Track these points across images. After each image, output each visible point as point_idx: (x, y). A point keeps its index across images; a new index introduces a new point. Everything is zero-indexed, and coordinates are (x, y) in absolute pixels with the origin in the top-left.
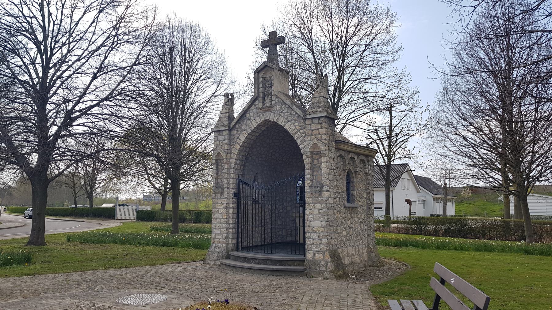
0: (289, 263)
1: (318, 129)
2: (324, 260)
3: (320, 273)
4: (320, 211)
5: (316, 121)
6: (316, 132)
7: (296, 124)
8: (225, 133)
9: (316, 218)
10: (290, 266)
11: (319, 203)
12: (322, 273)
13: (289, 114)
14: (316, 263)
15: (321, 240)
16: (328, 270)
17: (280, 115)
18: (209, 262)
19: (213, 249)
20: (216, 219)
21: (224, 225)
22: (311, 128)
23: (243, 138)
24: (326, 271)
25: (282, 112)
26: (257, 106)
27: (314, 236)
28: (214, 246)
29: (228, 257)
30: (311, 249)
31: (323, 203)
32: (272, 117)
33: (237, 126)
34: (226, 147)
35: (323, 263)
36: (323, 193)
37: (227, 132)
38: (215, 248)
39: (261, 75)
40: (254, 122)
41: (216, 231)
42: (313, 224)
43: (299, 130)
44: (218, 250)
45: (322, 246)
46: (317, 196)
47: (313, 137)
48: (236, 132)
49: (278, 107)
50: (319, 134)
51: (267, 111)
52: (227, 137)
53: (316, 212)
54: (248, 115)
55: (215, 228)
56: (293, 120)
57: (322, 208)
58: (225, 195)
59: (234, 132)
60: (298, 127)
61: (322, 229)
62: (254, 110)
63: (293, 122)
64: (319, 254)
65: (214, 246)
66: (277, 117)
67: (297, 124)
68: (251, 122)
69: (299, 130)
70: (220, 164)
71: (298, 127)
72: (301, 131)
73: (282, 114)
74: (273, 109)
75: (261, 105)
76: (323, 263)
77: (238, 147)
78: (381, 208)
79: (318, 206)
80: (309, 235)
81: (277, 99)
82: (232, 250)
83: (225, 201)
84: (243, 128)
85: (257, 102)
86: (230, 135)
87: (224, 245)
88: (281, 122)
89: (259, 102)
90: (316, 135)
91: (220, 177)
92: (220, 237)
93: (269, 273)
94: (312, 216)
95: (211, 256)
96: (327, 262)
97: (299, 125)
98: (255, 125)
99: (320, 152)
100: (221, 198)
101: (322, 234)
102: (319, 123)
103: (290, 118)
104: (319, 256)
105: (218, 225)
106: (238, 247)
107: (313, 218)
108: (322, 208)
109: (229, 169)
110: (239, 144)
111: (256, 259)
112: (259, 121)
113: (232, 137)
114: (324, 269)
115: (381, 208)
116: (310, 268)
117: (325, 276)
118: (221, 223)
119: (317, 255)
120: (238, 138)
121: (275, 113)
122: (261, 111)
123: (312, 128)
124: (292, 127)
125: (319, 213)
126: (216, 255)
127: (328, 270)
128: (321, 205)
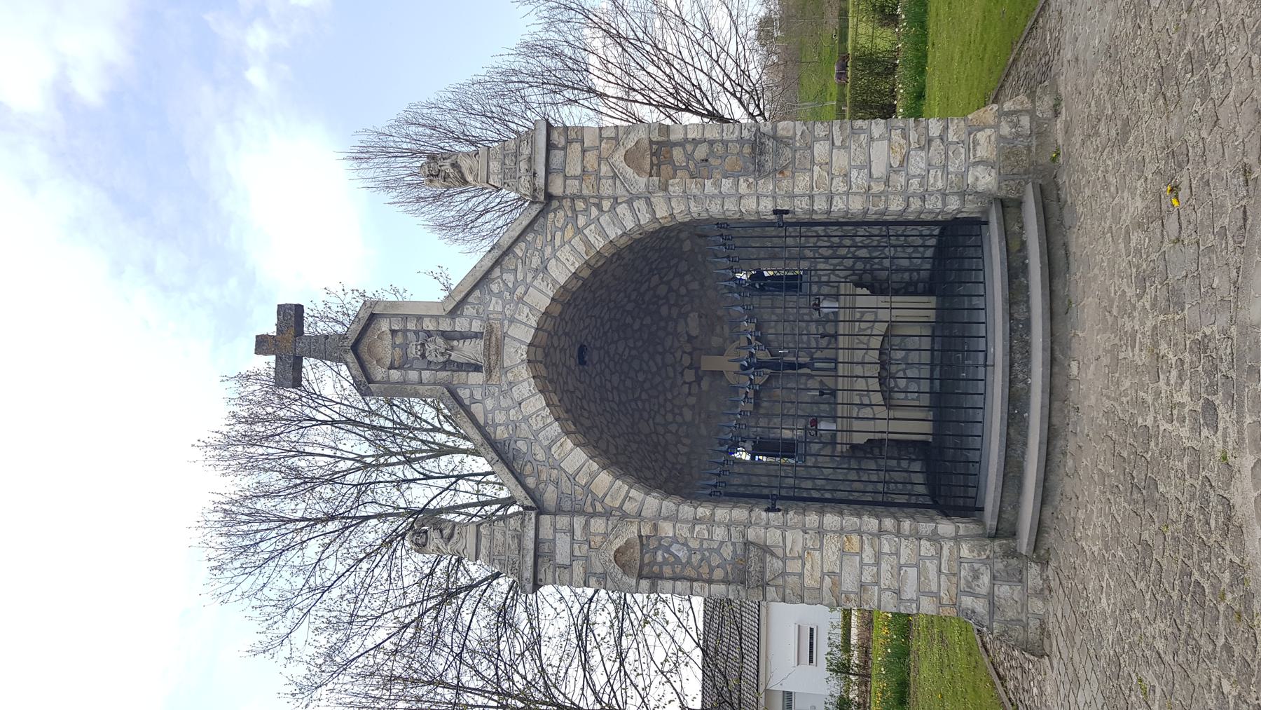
0: (1015, 246)
1: (584, 151)
2: (997, 127)
3: (1040, 132)
4: (838, 143)
5: (557, 157)
6: (591, 157)
7: (558, 242)
8: (547, 532)
9: (860, 159)
10: (1023, 244)
11: (811, 148)
12: (1039, 125)
13: (524, 263)
14: (1007, 151)
15: (930, 141)
16: (1028, 105)
17: (521, 299)
18: (1034, 624)
19: (980, 606)
20: (862, 586)
21: (886, 549)
22: (575, 177)
23: (575, 458)
24: (1031, 113)
25: (512, 293)
26: (478, 396)
27: (917, 163)
28: (967, 601)
29: (1005, 531)
30: (963, 176)
31: (812, 132)
32: (522, 333)
33: (531, 482)
34: (598, 525)
35: (1006, 130)
36: (780, 133)
37: (546, 520)
38: (976, 596)
39: (379, 373)
40: (523, 405)
41: (910, 592)
42: (879, 169)
43: (578, 231)
44: (985, 579)
45: (952, 137)
46: (788, 152)
47: (605, 169)
48: (551, 488)
49: (495, 306)
50: (598, 148)
51: (499, 352)
52: (563, 521)
53: (840, 160)
54: (501, 434)
55: (898, 592)
56: (542, 251)
57: (829, 138)
58: (774, 537)
59: (550, 496)
60: (569, 232)
61: (896, 136)
62: (489, 403)
63: (549, 250)
64: (976, 143)
65: (967, 601)
66: (526, 310)
67: (558, 234)
68: (526, 419)
69: (578, 231)
70: (656, 569)
71: (569, 232)
72: (582, 221)
73: (520, 290)
74: (496, 325)
75: (476, 378)
76: (1006, 130)
77: (605, 478)
78: (812, 630)
79: (820, 149)
80: (915, 181)
81: (469, 310)
82: (981, 522)
83: (795, 541)
84: (541, 456)
85: (464, 394)
86: (559, 511)
87: (965, 552)
88: (541, 297)
89: (465, 385)
90: (600, 158)
91: (705, 570)
92: (931, 567)
93: (1058, 284)
94: (854, 173)
95: (1010, 614)
96: (1001, 114)
97: (563, 229)
99: (651, 142)
100: (784, 560)
101: (913, 136)
102: (564, 148)
103: (535, 262)
104: (985, 145)
105: (886, 580)
107: (861, 168)
108: (829, 138)
109: (674, 519)
110: (593, 476)
111: (1011, 366)
113: (567, 505)
114: (1025, 121)
115: (812, 630)
116: (1026, 172)
117: (1049, 114)
118: (877, 563)
119: (983, 151)
120: (572, 478)
121: (512, 321)
122: (496, 375)
123: (578, 172)
125: (843, 147)
126: (1003, 591)
127: (1028, 105)
128: (818, 140)
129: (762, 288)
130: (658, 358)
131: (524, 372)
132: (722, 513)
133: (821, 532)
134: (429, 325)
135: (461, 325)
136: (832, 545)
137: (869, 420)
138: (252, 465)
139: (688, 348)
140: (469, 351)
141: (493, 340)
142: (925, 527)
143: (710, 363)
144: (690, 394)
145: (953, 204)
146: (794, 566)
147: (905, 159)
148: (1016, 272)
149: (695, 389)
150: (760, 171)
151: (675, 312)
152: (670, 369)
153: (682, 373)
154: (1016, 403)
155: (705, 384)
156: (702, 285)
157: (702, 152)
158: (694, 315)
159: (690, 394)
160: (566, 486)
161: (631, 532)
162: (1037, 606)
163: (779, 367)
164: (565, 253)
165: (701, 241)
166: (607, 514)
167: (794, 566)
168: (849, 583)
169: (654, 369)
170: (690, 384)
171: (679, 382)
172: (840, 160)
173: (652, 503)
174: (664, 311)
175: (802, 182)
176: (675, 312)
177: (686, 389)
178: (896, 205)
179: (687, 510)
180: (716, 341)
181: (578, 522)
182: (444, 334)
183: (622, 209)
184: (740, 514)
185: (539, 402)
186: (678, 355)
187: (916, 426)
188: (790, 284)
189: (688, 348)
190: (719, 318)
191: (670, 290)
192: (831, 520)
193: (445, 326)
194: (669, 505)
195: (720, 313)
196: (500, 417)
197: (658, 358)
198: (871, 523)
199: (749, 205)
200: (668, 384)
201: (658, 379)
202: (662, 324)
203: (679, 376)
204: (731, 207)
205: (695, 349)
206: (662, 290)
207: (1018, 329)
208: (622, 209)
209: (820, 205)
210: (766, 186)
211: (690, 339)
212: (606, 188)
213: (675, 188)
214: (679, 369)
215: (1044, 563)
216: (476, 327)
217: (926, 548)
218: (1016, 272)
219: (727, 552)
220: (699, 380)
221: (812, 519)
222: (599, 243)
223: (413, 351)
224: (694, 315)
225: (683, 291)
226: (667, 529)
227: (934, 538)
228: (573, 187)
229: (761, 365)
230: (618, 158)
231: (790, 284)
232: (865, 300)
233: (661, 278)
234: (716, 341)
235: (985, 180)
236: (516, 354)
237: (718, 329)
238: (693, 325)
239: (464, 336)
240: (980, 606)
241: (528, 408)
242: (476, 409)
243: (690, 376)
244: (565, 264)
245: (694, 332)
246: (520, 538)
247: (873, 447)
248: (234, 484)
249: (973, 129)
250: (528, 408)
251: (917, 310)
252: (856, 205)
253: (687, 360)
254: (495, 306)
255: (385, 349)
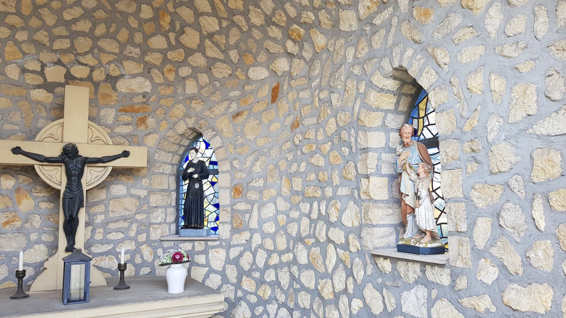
129: (186, 176)
130: (84, 26)
139: (98, 75)
143: (77, 99)
144: (24, 71)
149: (30, 79)
151: (154, 58)
152: (65, 44)
153: (59, 62)
155: (40, 95)
156: (192, 98)
158: (147, 86)
159: (24, 71)
163: (71, 205)
165: (266, 92)
169: (67, 16)
170: (42, 73)
171: (46, 57)
174: (158, 42)
176: (154, 58)
177: (35, 66)
180: (109, 115)
186: (89, 60)
188: (192, 214)
189: (98, 75)
190: (143, 121)
191: (189, 52)
195: (150, 121)
197: (84, 26)
200: (41, 36)
201: (50, 20)
202: (138, 38)
203: (55, 57)
205: (96, 85)
206: (191, 39)
211: (112, 80)
214: (66, 59)
220: (49, 87)
224: (147, 86)
225: (185, 71)
229: (74, 178)
231: (192, 214)
233: (211, 36)
234: (109, 115)
237: (126, 118)
238: (134, 85)
245: (122, 86)
253: (79, 72)
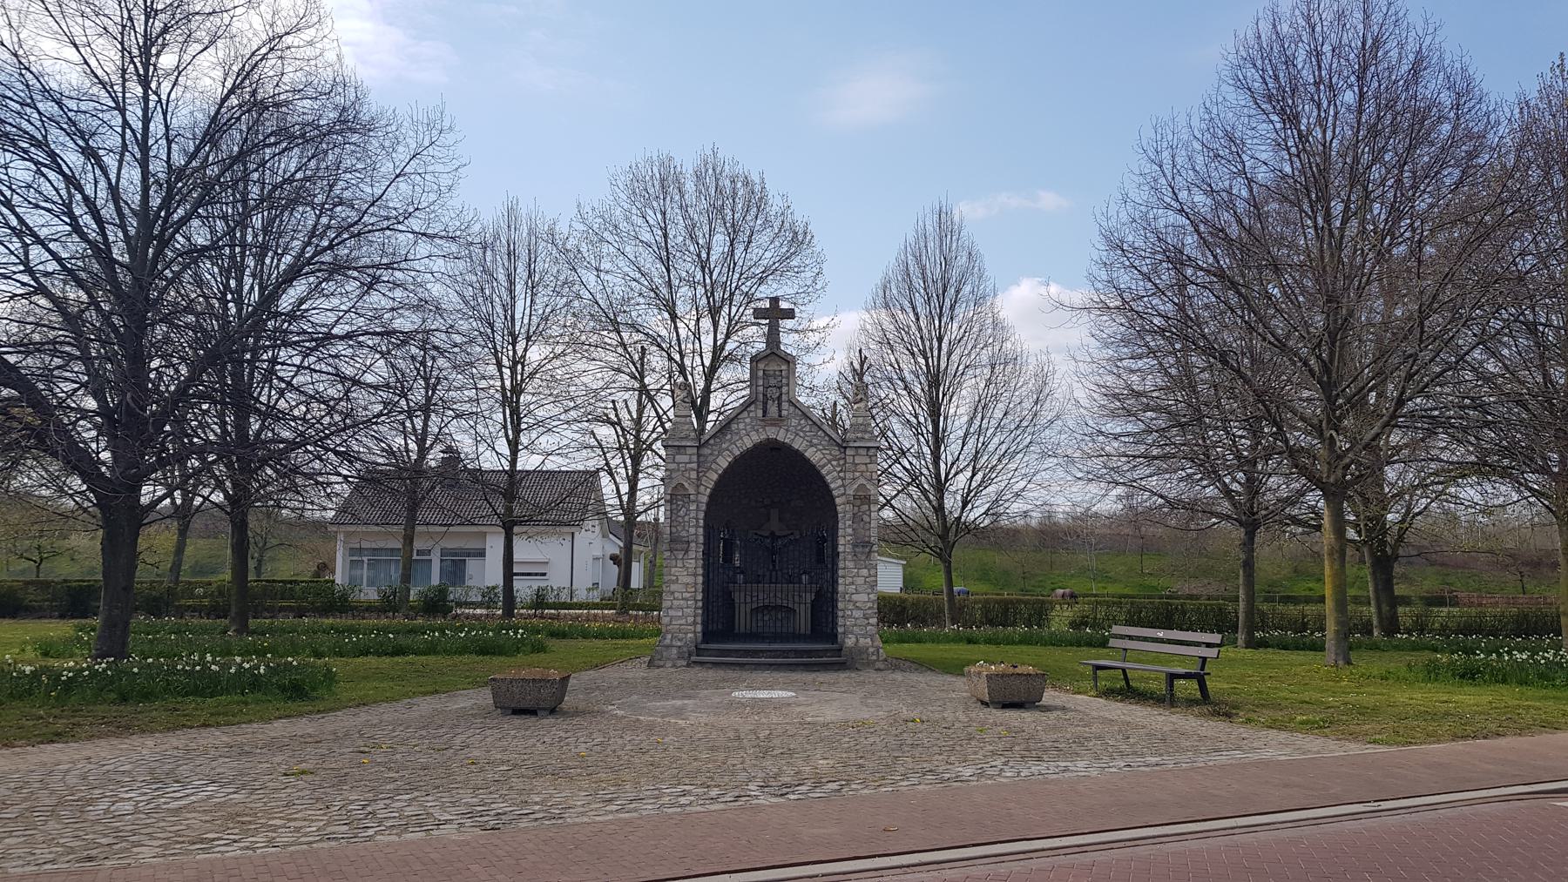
3: (870, 664)
8: (689, 451)
19: (668, 641)
23: (724, 463)
27: (857, 614)
29: (699, 652)
32: (781, 436)
34: (694, 475)
39: (761, 366)
40: (748, 438)
41: (671, 613)
42: (854, 597)
49: (794, 422)
52: (695, 458)
53: (860, 581)
54: (734, 426)
58: (692, 554)
59: (706, 451)
75: (760, 413)
77: (715, 477)
85: (752, 408)
86: (699, 456)
88: (798, 444)
98: (748, 443)
106: (708, 635)
109: (698, 509)
112: (756, 438)
124: (819, 455)
126: (675, 651)
131: (763, 437)
132: (701, 531)
133: (695, 575)
134: (784, 389)
135: (785, 405)
136: (690, 580)
137: (745, 601)
138: (699, 177)
140: (773, 409)
141: (779, 420)
142: (699, 619)
145: (840, 630)
146: (680, 564)
147: (858, 608)
148: (809, 653)
150: (855, 546)
154: (755, 653)
157: (866, 518)
160: (711, 458)
161: (691, 491)
162: (669, 664)
164: (819, 455)
166: (698, 479)
167: (680, 564)
168: (673, 587)
172: (860, 581)
173: (705, 499)
175: (850, 565)
178: (840, 605)
179: (702, 515)
181: (694, 466)
182: (779, 398)
183: (839, 482)
184: (701, 539)
185: (749, 444)
187: (742, 621)
192: (700, 579)
193: (784, 397)
194: (704, 507)
196: (741, 426)
198: (700, 597)
199: (841, 541)
204: (841, 532)
207: (785, 653)
208: (839, 482)
209: (841, 572)
210: (849, 549)
212: (850, 475)
213: (848, 507)
215: (688, 665)
216: (784, 413)
217: (691, 620)
218: (809, 653)
219: (684, 534)
221: (700, 571)
222: (824, 472)
223: (772, 382)
226: (693, 507)
227: (695, 623)
228: (849, 459)
230: (862, 481)
232: (809, 597)
235: (850, 642)
236: (771, 433)
239: (779, 405)
240: (668, 641)
241: (746, 439)
242: (745, 414)
243: (767, 501)
244: (814, 455)
246: (686, 438)
247: (730, 604)
248: (688, 169)
249: (872, 637)
250: (746, 439)
251: (803, 621)
252: (841, 588)
254: (794, 422)
255: (773, 367)
